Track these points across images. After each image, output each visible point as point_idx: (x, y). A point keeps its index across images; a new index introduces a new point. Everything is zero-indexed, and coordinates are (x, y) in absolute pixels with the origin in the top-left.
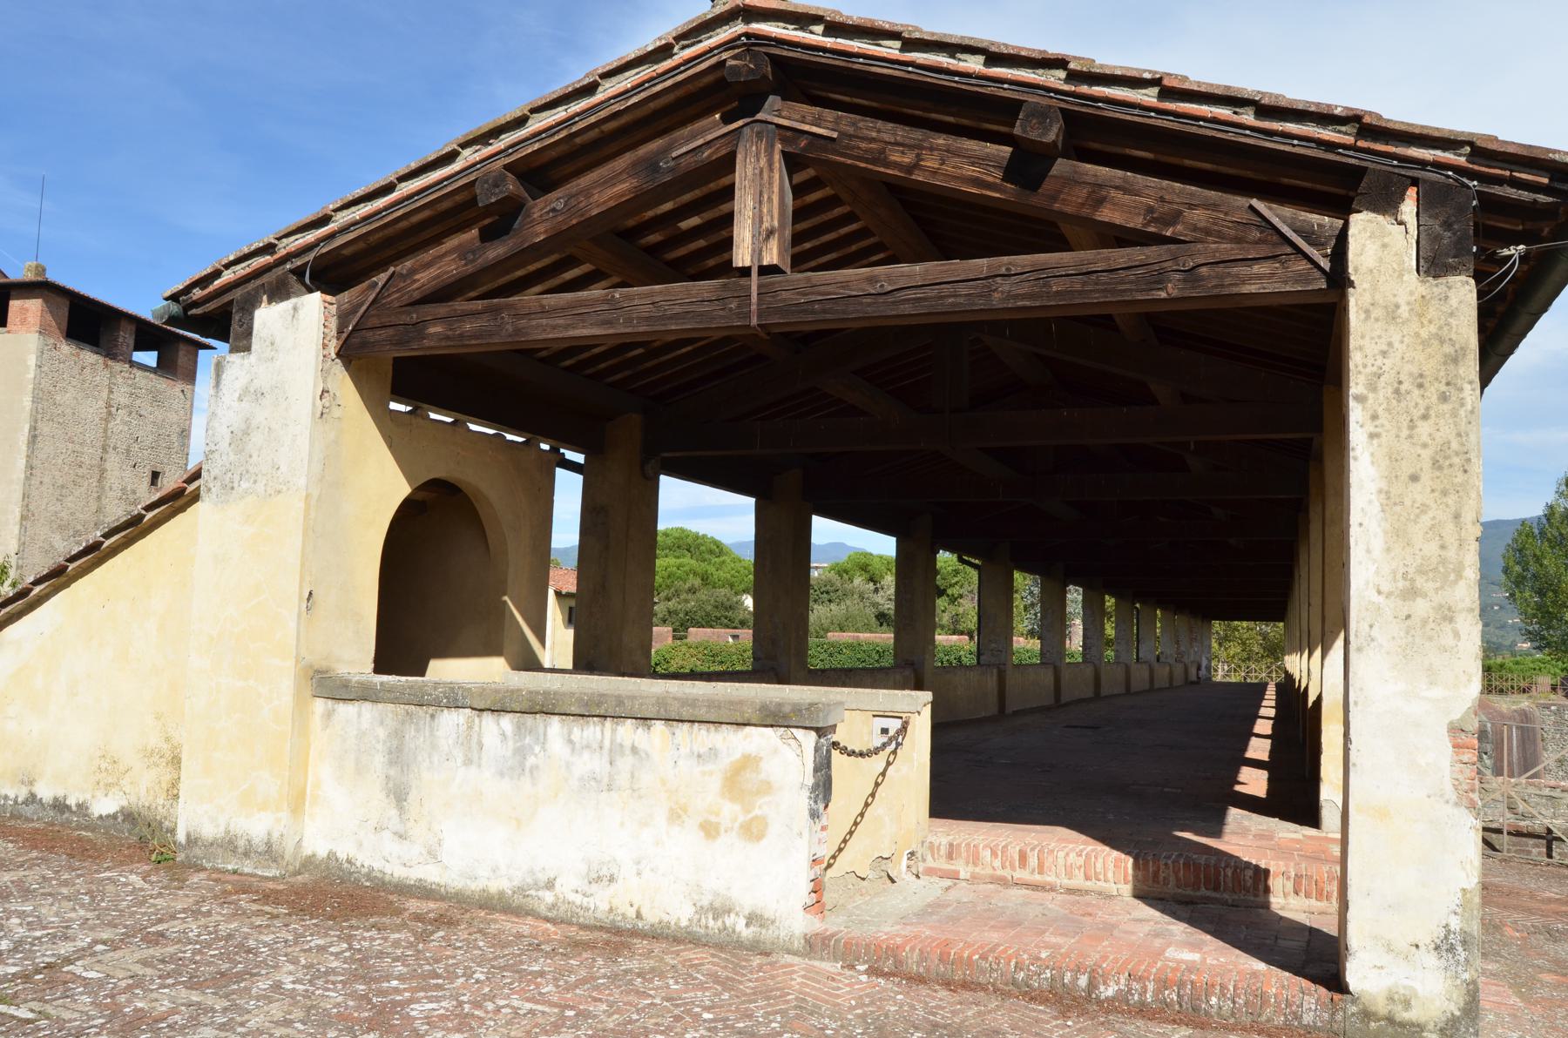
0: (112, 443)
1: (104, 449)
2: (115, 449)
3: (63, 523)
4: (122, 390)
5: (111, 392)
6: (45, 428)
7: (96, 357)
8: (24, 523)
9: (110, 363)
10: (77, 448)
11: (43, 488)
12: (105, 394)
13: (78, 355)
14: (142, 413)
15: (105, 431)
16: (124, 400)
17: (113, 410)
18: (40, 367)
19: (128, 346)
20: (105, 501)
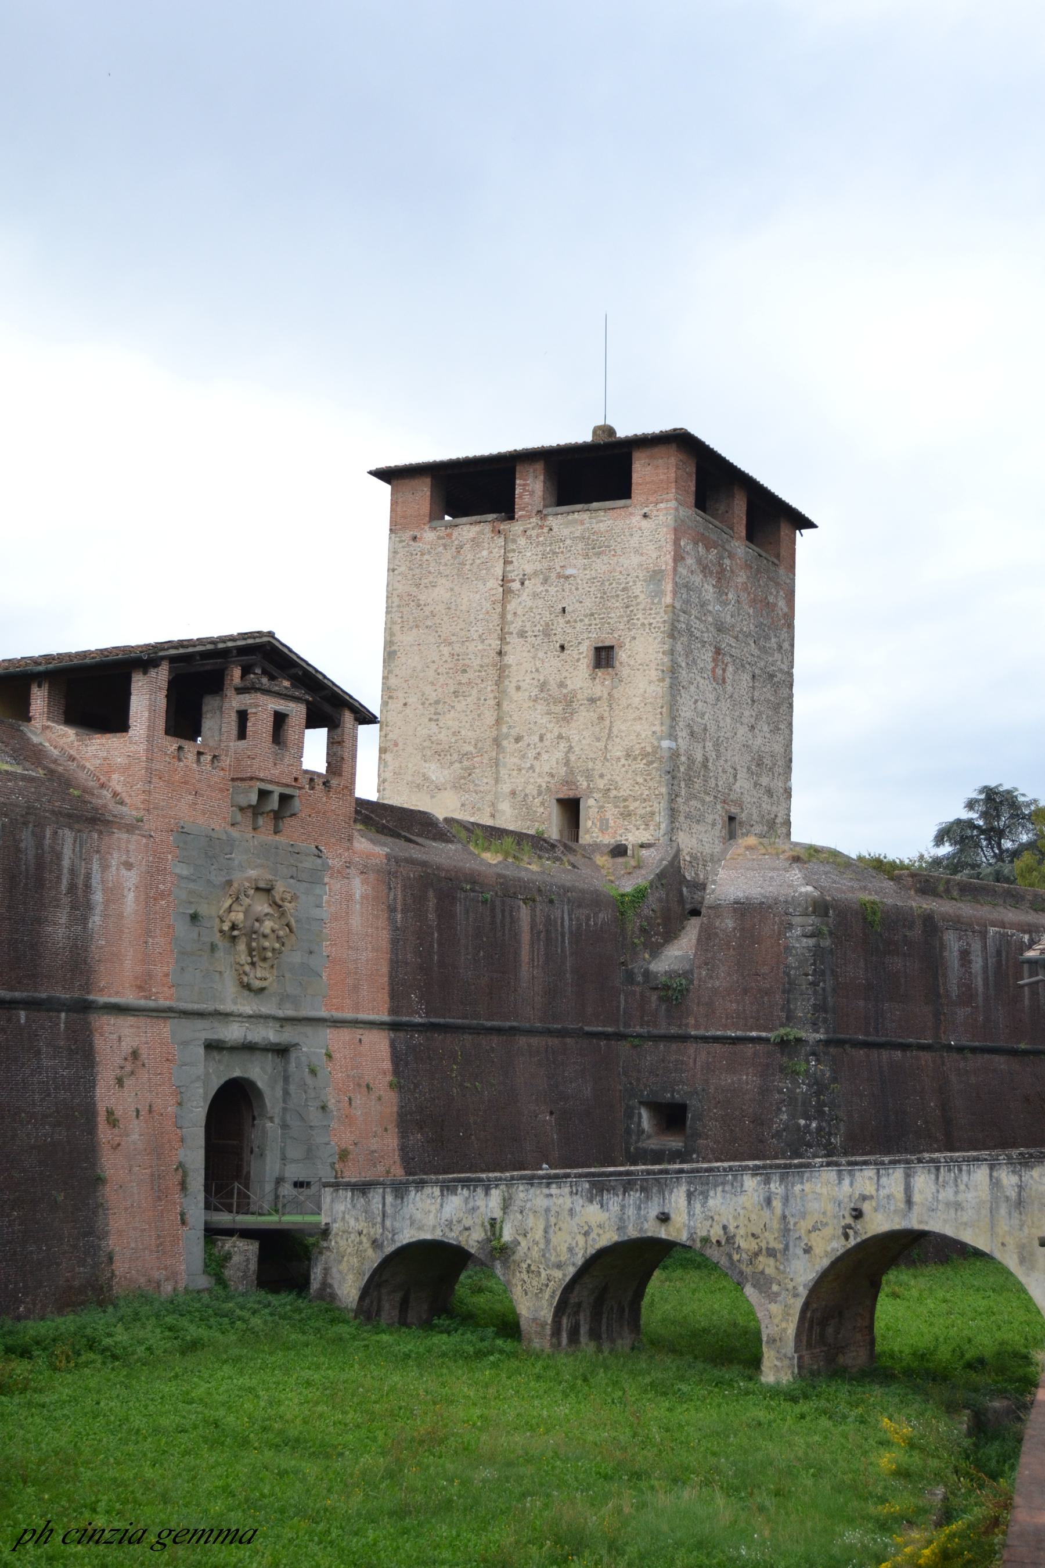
0: (514, 628)
1: (502, 639)
2: (522, 634)
3: (440, 747)
4: (529, 554)
5: (507, 562)
6: (406, 639)
7: (476, 529)
8: (383, 756)
9: (503, 526)
10: (457, 648)
11: (408, 711)
12: (499, 571)
13: (449, 535)
14: (569, 571)
15: (503, 616)
16: (529, 569)
17: (516, 585)
18: (394, 570)
19: (532, 493)
20: (506, 706)
